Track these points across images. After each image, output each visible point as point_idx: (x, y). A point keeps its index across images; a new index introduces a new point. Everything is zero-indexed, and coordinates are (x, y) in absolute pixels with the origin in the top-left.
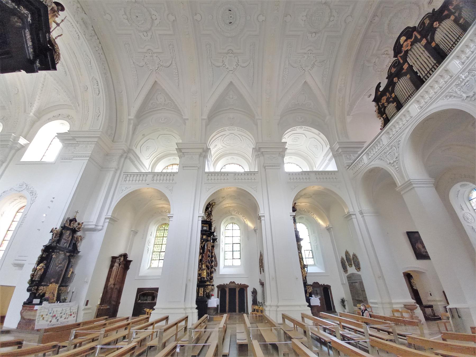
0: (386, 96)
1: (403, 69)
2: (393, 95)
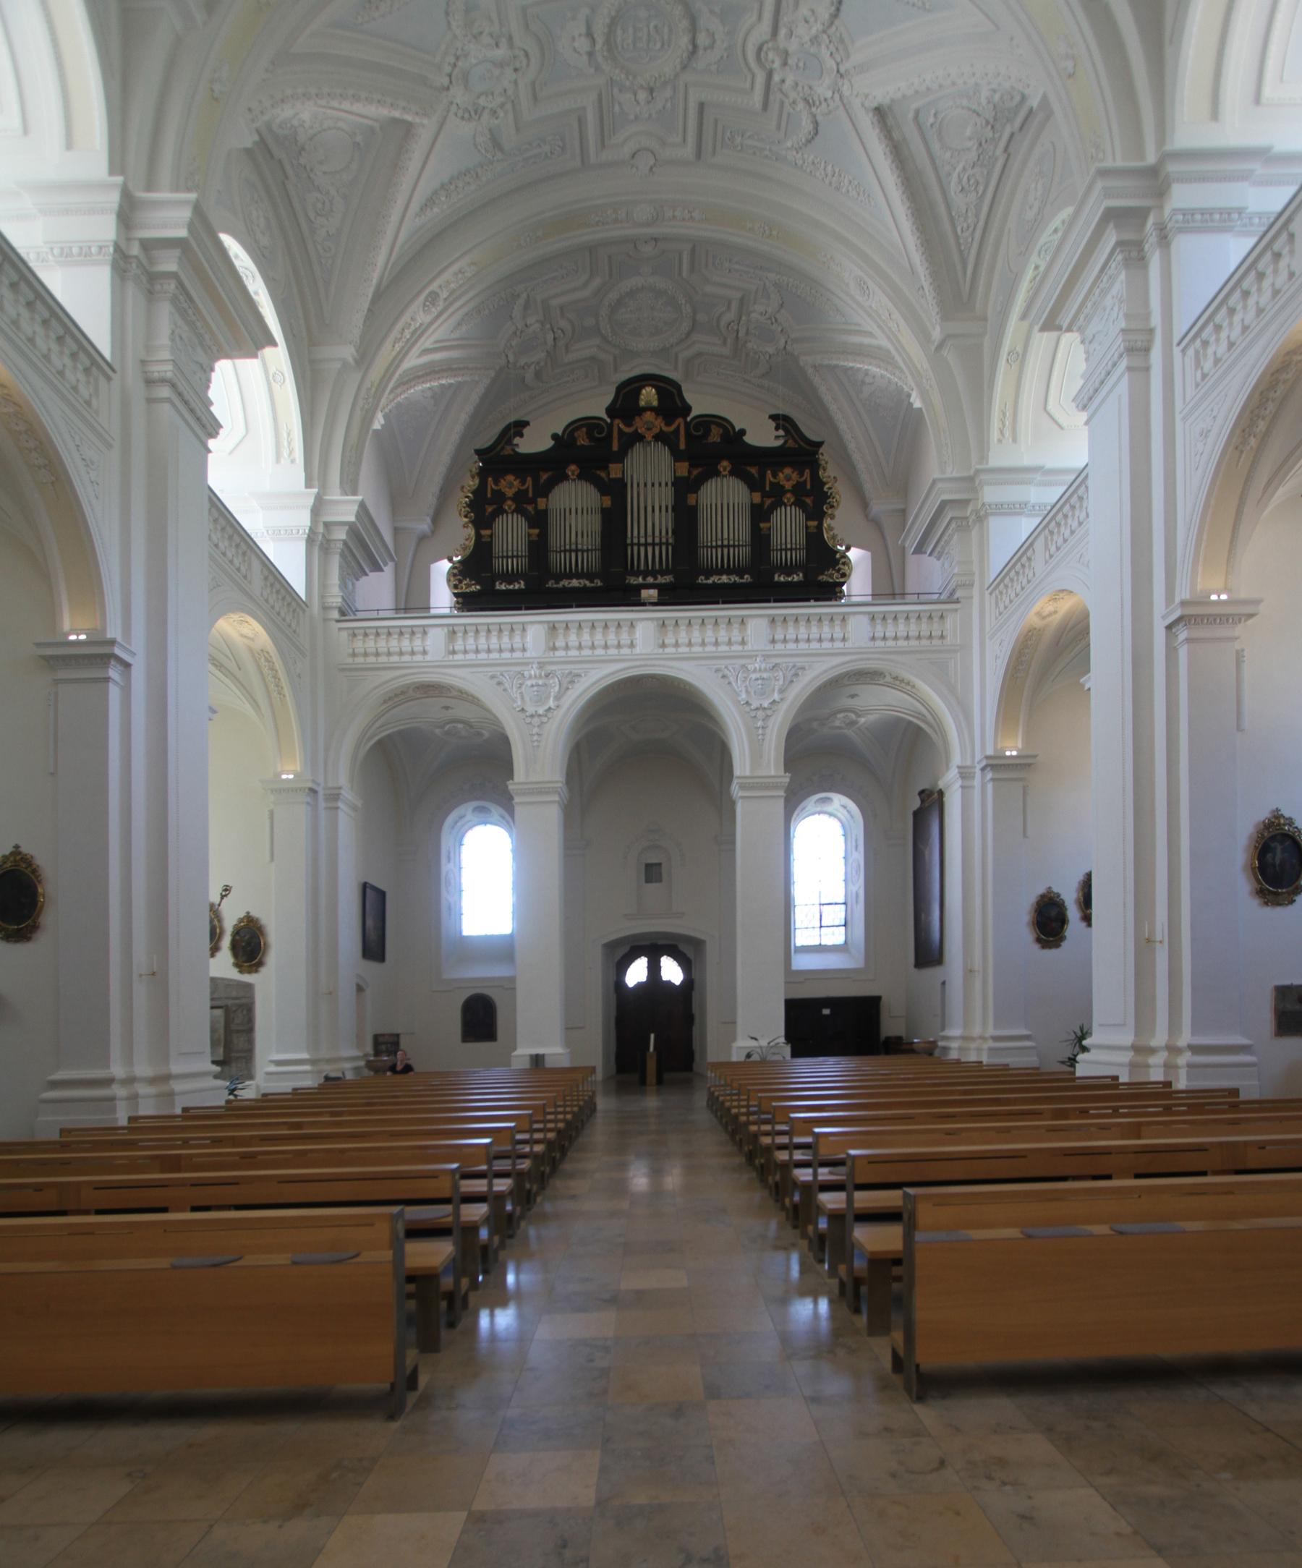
0: (523, 482)
1: (606, 468)
2: (541, 503)
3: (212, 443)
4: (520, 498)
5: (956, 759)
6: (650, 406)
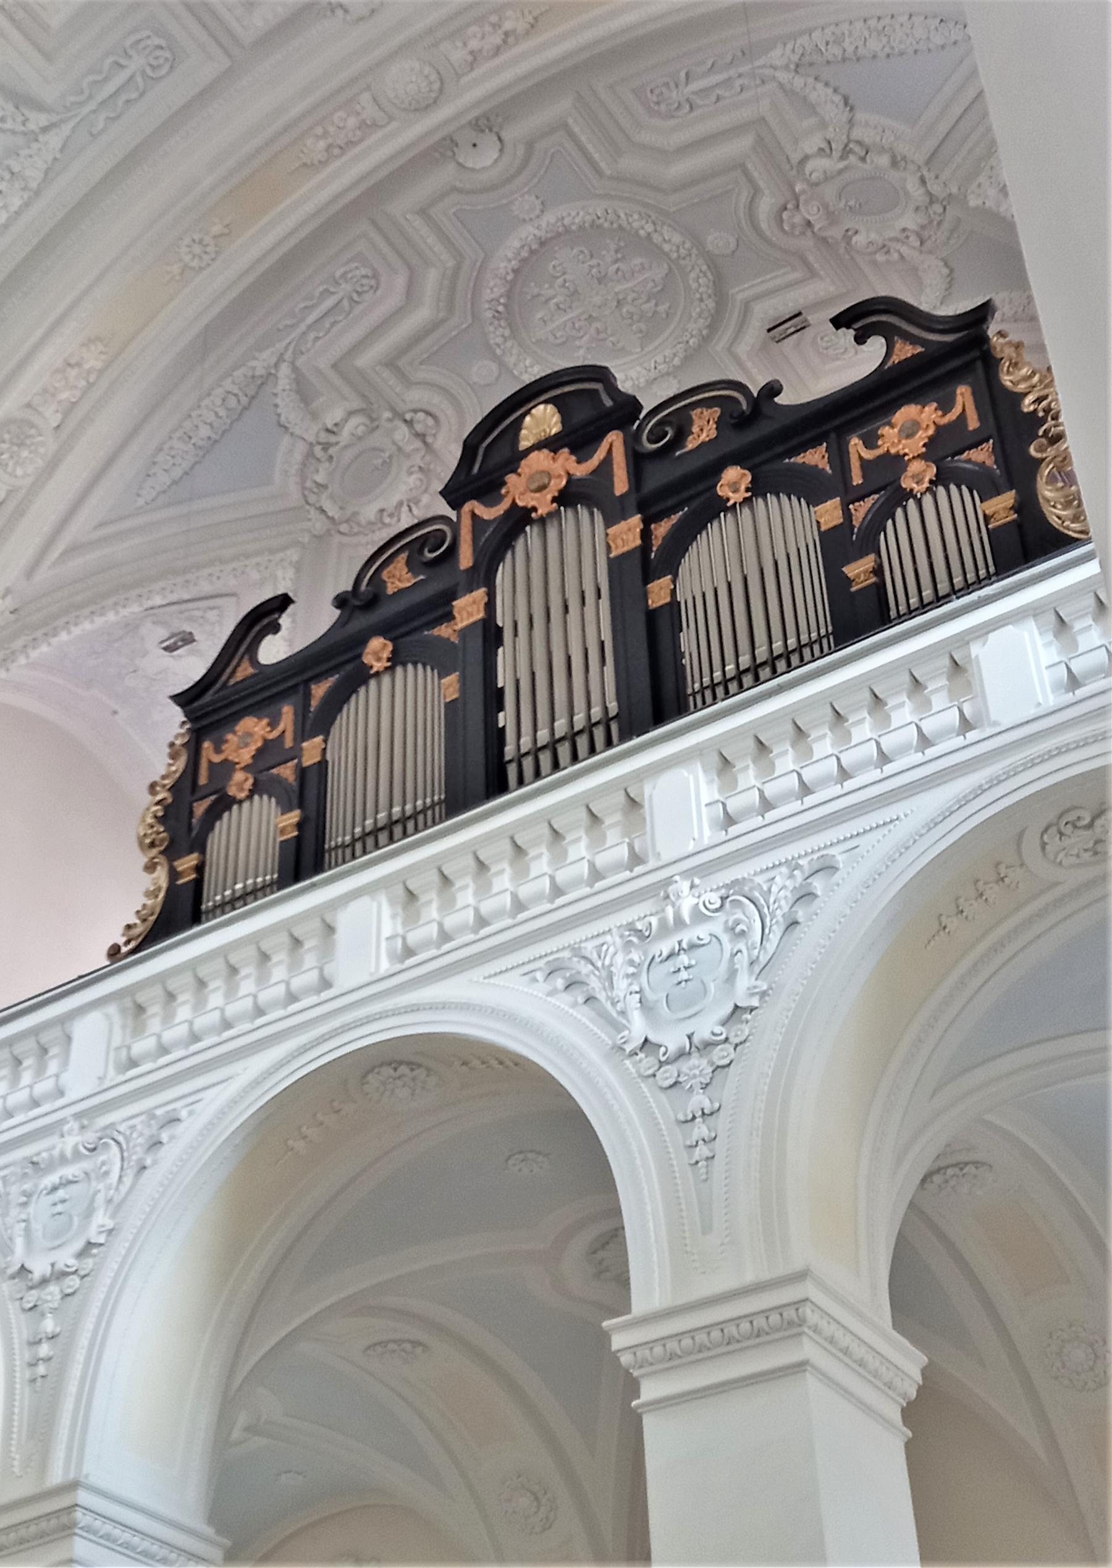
1: (449, 617)
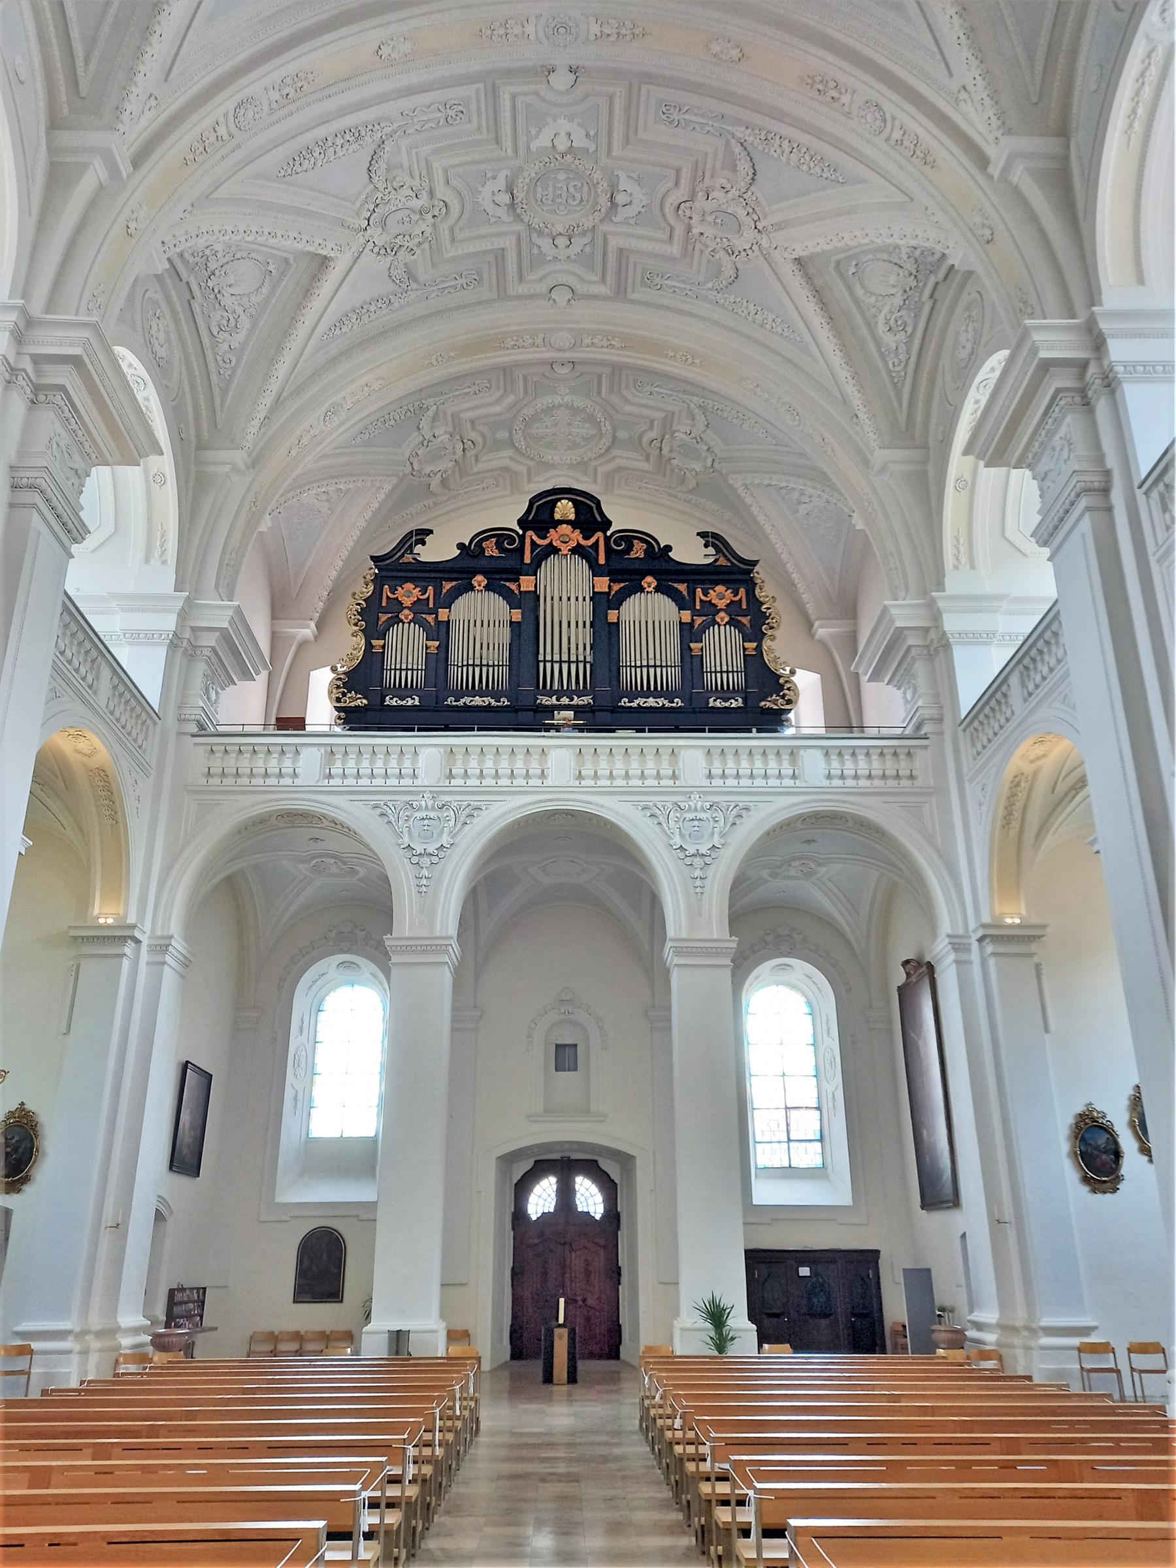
2: (443, 614)
3: (75, 549)
4: (419, 607)
5: (945, 927)
6: (565, 517)
